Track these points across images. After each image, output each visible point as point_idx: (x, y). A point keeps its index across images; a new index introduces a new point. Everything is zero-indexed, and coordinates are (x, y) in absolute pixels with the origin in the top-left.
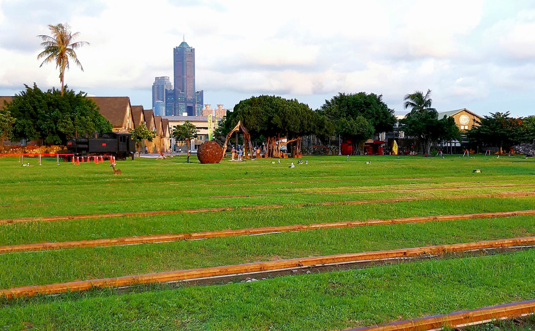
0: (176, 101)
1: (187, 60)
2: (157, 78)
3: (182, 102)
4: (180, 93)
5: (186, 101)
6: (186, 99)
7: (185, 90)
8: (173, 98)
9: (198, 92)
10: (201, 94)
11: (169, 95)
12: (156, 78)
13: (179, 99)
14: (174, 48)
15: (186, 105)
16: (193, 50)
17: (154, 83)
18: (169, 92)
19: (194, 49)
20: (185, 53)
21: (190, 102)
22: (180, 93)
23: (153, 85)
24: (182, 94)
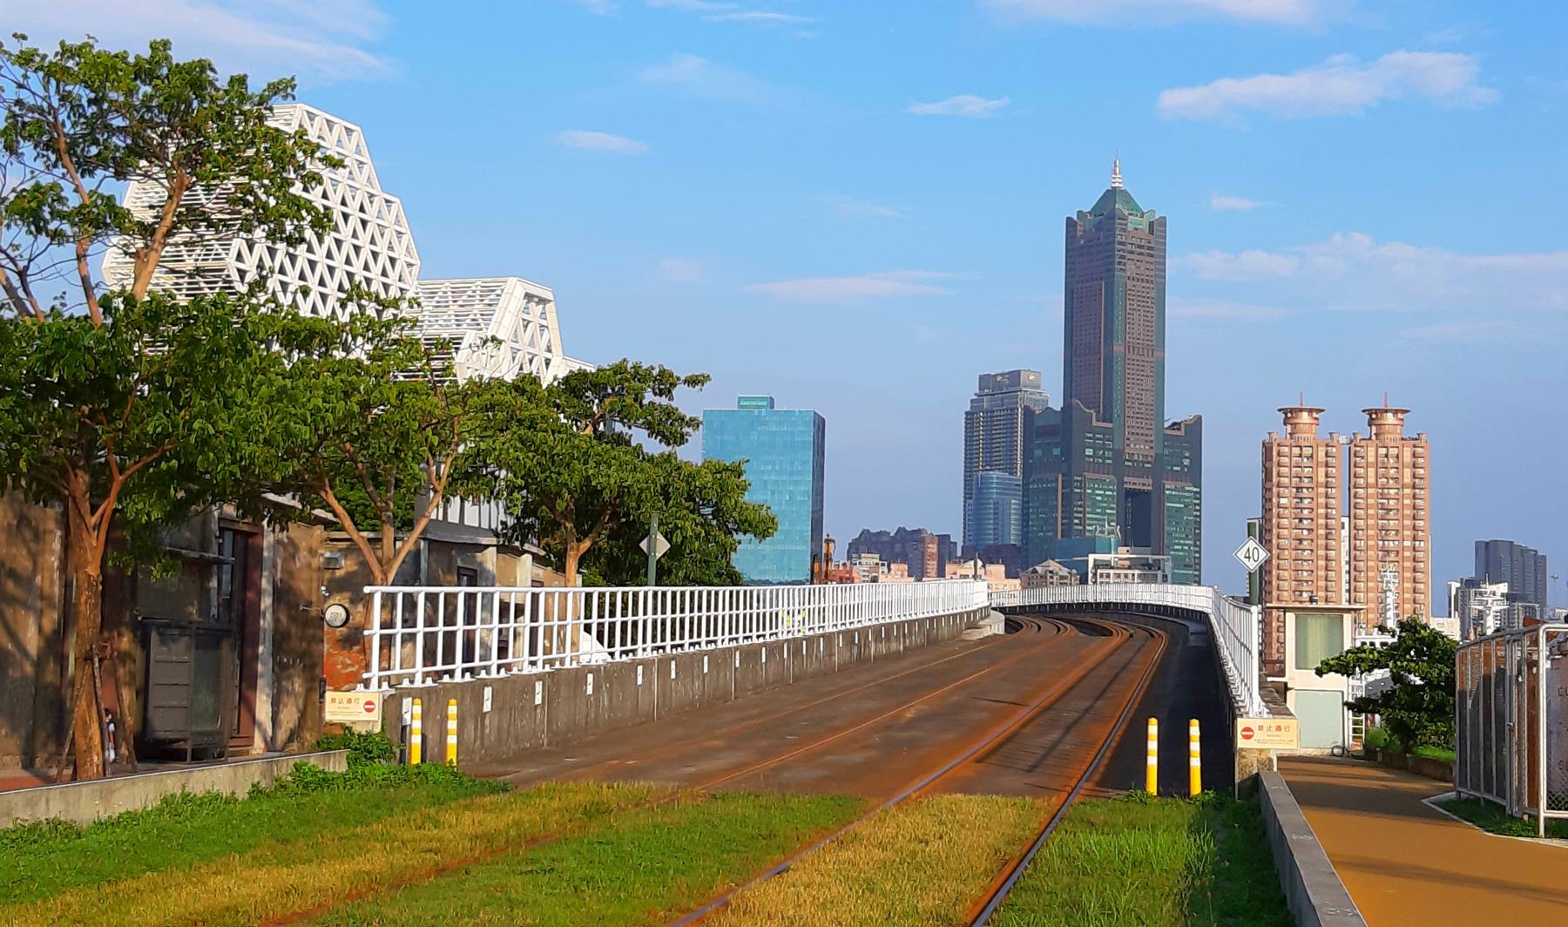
0: (1068, 463)
1: (1131, 268)
2: (985, 380)
3: (1100, 468)
4: (1095, 423)
5: (1119, 464)
6: (1118, 455)
7: (1116, 411)
8: (1057, 451)
9: (1175, 424)
10: (1192, 432)
11: (1038, 435)
12: (981, 377)
13: (1089, 452)
14: (1069, 219)
15: (1121, 483)
16: (1157, 228)
17: (972, 401)
18: (1039, 423)
19: (1162, 222)
20: (1118, 238)
21: (1138, 471)
22: (1095, 423)
23: (968, 409)
24: (1105, 431)
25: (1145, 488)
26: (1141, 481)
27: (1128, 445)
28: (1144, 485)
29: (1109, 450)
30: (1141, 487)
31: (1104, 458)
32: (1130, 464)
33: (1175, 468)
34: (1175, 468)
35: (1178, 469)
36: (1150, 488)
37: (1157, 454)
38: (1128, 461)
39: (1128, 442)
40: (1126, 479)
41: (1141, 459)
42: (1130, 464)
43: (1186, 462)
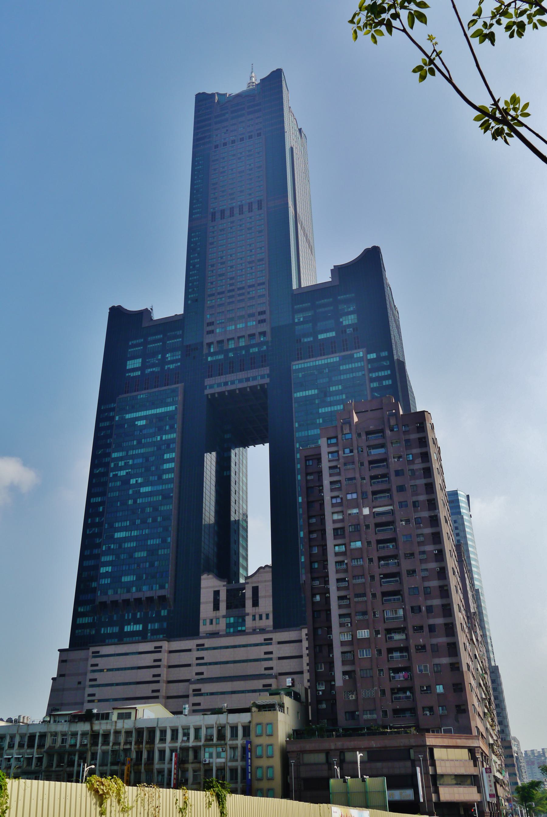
25: (252, 383)
26: (242, 375)
27: (212, 332)
28: (248, 380)
29: (173, 350)
30: (245, 385)
31: (164, 362)
32: (221, 357)
33: (321, 337)
34: (321, 337)
35: (333, 334)
36: (267, 380)
37: (272, 329)
38: (215, 354)
39: (210, 328)
40: (208, 382)
41: (242, 343)
42: (221, 357)
43: (349, 320)
